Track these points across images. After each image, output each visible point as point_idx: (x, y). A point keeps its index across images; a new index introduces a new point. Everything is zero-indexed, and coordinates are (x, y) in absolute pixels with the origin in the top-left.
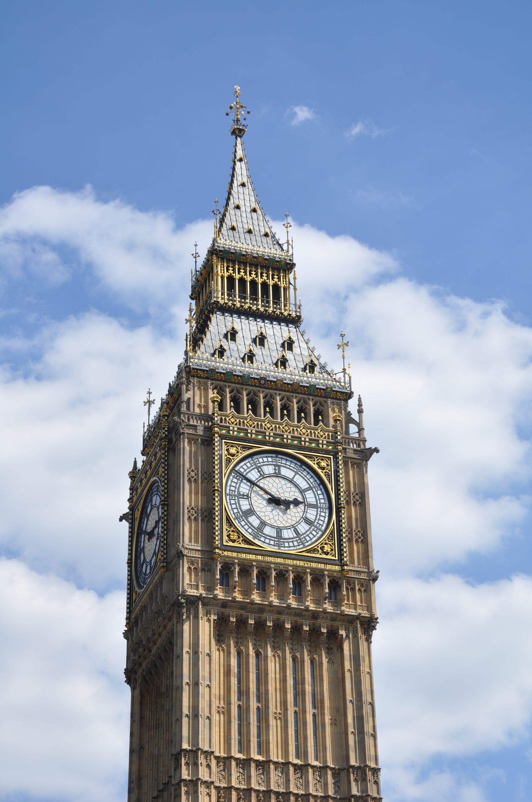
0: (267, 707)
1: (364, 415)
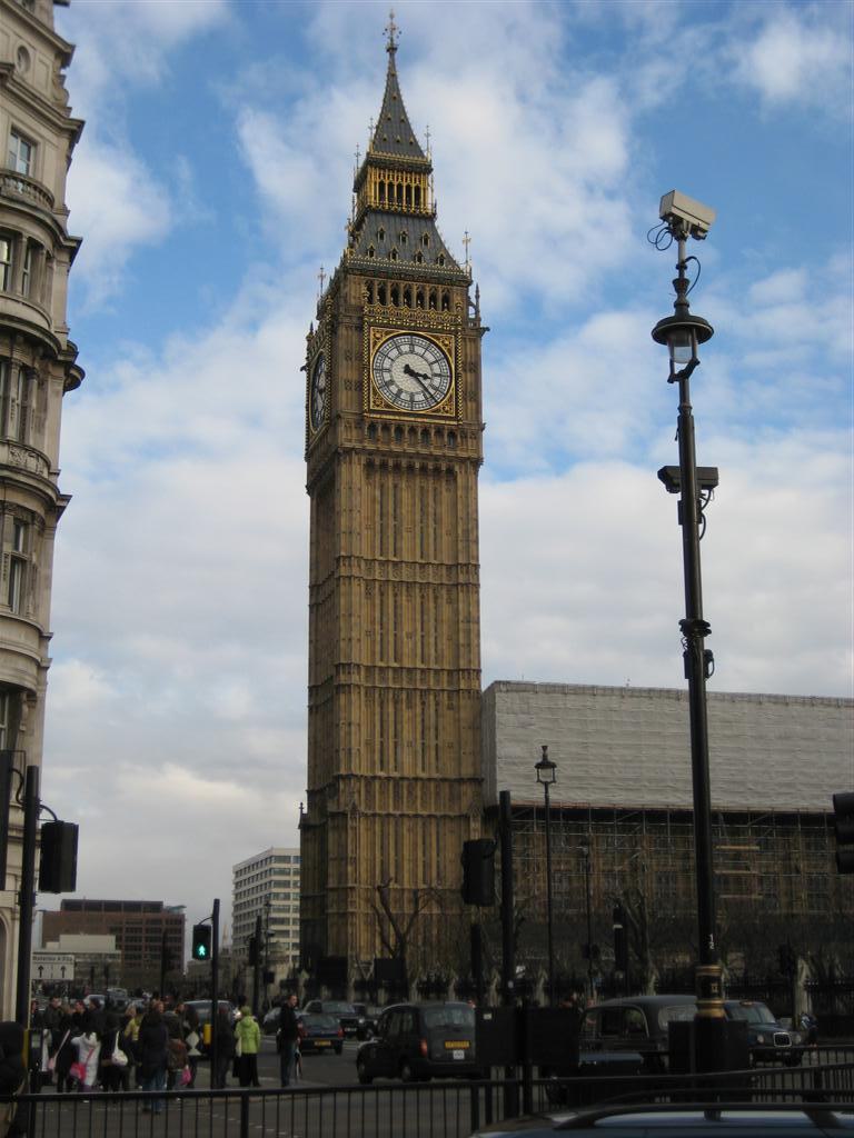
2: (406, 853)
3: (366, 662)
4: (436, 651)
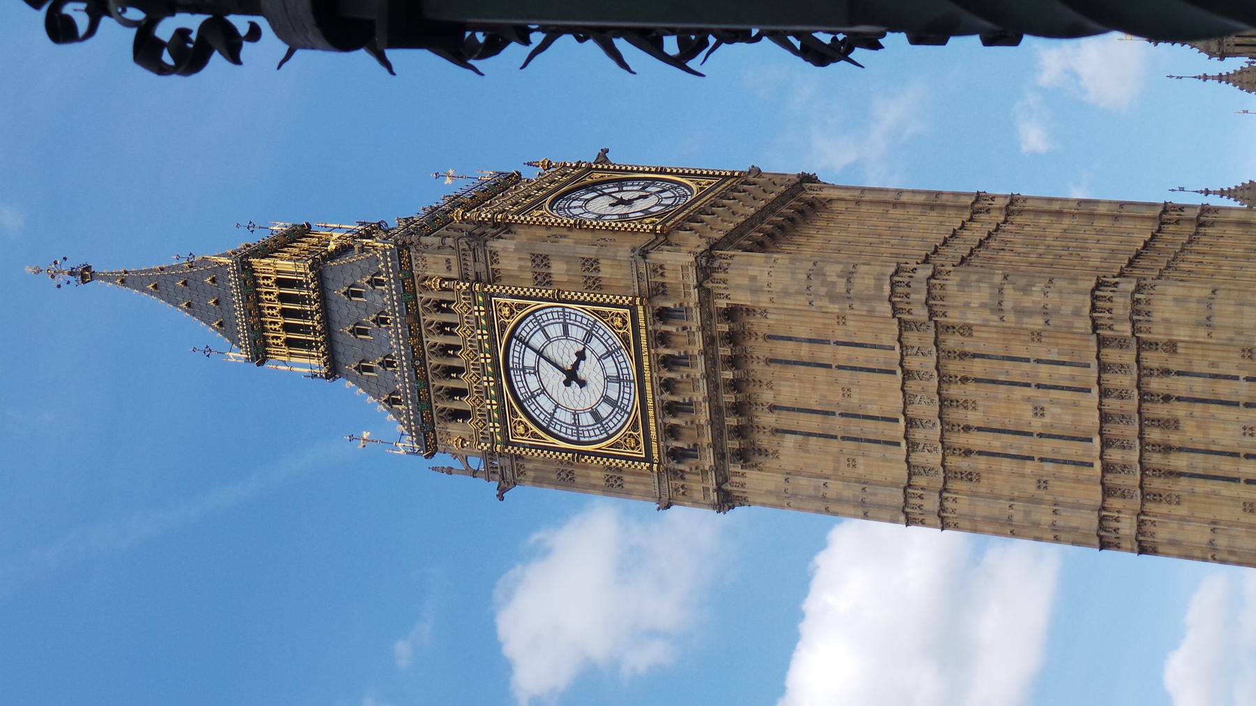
3: (1096, 495)
4: (1064, 363)
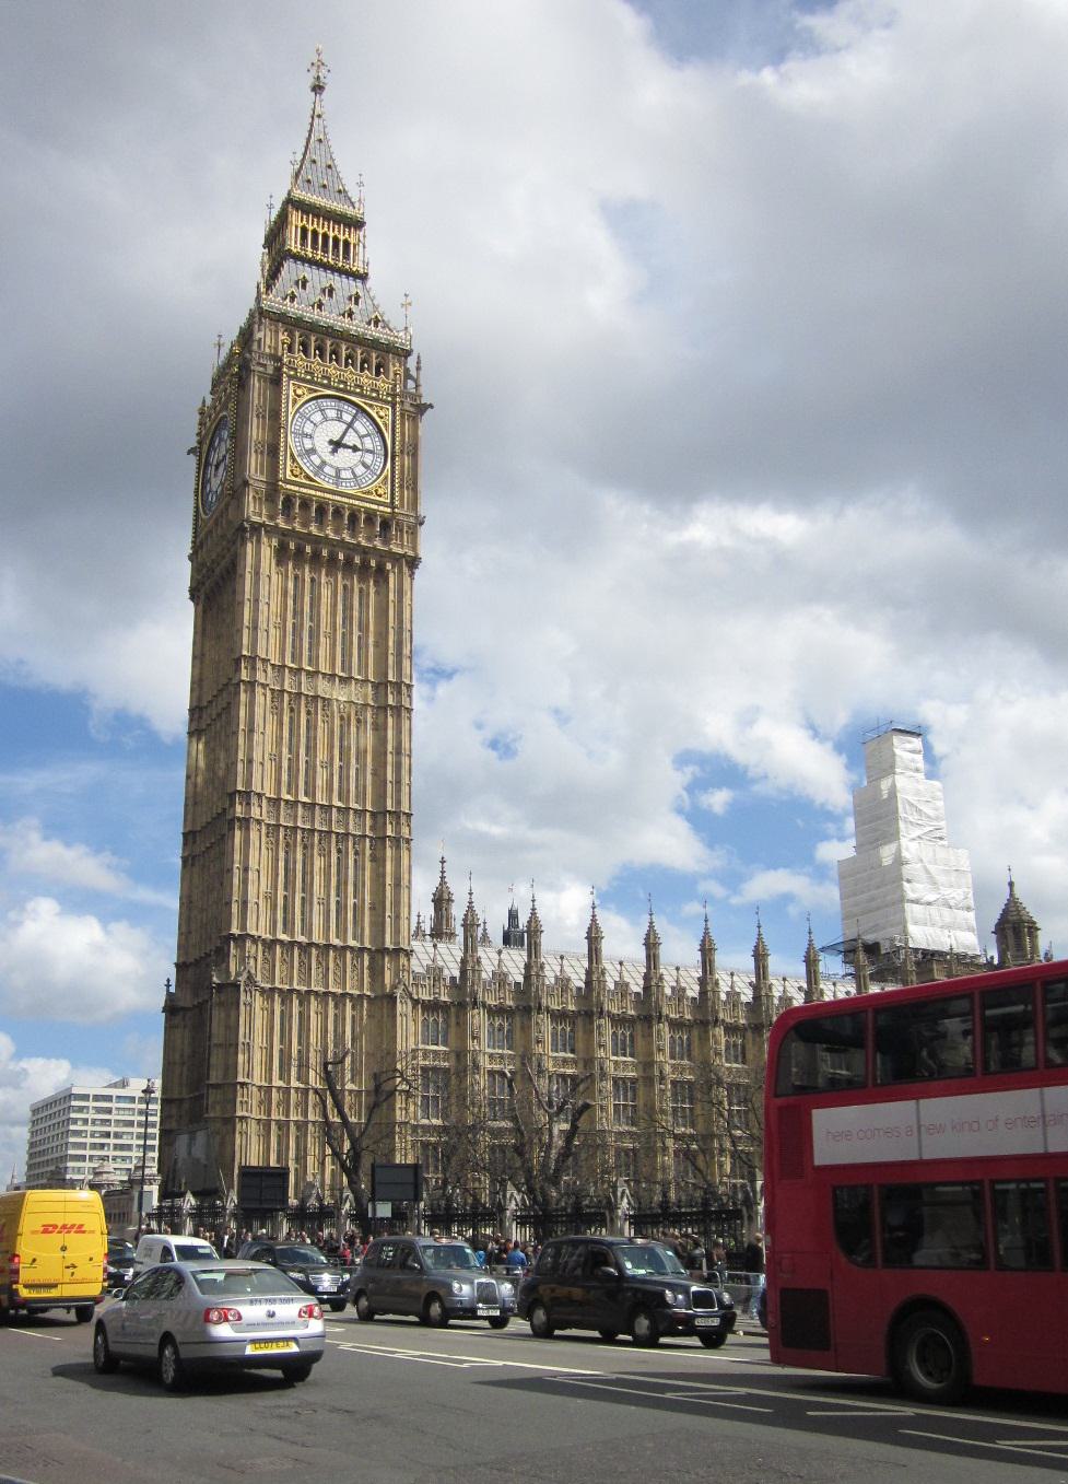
0: (319, 626)
1: (422, 372)
2: (313, 1040)
